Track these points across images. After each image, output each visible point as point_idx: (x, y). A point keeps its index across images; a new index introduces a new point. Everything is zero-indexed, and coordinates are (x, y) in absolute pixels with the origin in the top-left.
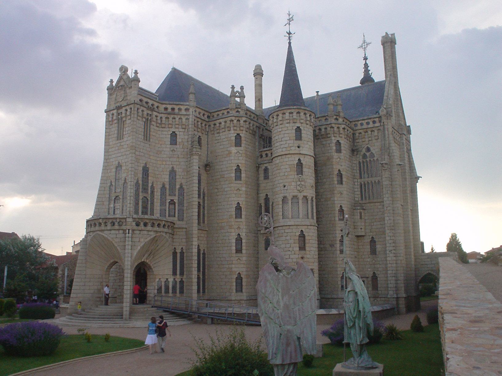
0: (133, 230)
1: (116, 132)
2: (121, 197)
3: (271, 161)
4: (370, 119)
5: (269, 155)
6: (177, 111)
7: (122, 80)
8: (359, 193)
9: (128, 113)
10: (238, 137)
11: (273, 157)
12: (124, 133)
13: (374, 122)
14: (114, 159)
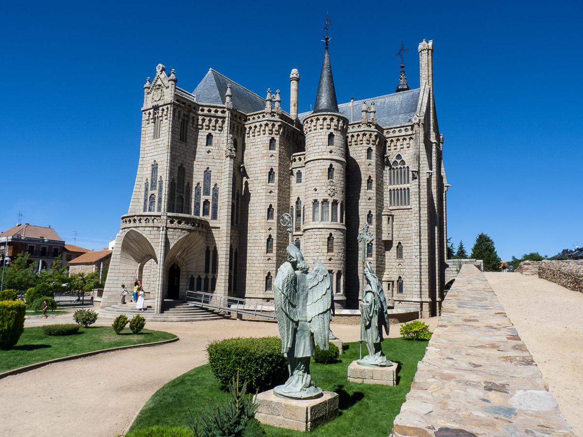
0: (167, 228)
1: (153, 131)
2: (157, 195)
3: (304, 165)
4: (403, 127)
5: (303, 160)
6: (214, 113)
7: (159, 79)
8: (388, 199)
9: (165, 113)
10: (272, 140)
11: (306, 161)
12: (161, 133)
14: (149, 158)
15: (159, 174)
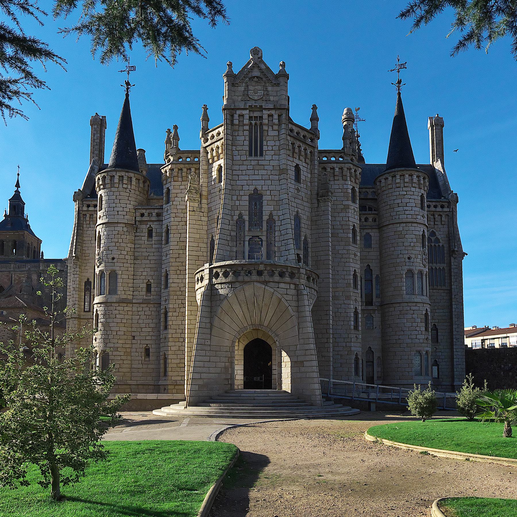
2: (264, 238)
13: (442, 207)
15: (267, 209)
